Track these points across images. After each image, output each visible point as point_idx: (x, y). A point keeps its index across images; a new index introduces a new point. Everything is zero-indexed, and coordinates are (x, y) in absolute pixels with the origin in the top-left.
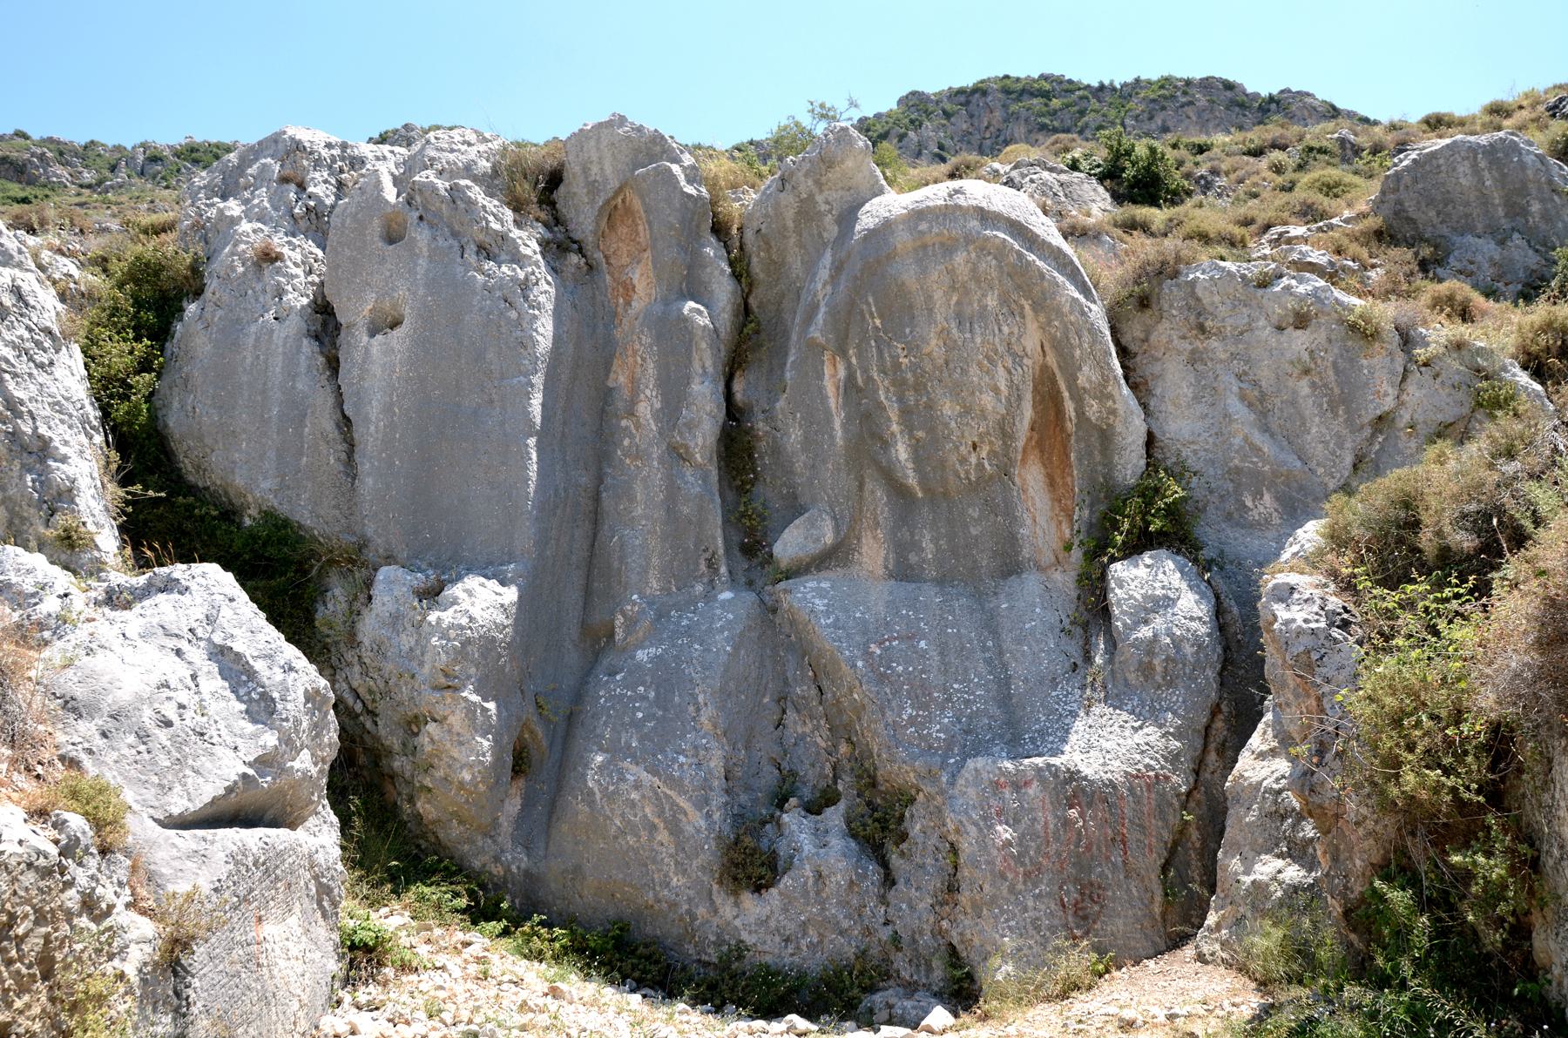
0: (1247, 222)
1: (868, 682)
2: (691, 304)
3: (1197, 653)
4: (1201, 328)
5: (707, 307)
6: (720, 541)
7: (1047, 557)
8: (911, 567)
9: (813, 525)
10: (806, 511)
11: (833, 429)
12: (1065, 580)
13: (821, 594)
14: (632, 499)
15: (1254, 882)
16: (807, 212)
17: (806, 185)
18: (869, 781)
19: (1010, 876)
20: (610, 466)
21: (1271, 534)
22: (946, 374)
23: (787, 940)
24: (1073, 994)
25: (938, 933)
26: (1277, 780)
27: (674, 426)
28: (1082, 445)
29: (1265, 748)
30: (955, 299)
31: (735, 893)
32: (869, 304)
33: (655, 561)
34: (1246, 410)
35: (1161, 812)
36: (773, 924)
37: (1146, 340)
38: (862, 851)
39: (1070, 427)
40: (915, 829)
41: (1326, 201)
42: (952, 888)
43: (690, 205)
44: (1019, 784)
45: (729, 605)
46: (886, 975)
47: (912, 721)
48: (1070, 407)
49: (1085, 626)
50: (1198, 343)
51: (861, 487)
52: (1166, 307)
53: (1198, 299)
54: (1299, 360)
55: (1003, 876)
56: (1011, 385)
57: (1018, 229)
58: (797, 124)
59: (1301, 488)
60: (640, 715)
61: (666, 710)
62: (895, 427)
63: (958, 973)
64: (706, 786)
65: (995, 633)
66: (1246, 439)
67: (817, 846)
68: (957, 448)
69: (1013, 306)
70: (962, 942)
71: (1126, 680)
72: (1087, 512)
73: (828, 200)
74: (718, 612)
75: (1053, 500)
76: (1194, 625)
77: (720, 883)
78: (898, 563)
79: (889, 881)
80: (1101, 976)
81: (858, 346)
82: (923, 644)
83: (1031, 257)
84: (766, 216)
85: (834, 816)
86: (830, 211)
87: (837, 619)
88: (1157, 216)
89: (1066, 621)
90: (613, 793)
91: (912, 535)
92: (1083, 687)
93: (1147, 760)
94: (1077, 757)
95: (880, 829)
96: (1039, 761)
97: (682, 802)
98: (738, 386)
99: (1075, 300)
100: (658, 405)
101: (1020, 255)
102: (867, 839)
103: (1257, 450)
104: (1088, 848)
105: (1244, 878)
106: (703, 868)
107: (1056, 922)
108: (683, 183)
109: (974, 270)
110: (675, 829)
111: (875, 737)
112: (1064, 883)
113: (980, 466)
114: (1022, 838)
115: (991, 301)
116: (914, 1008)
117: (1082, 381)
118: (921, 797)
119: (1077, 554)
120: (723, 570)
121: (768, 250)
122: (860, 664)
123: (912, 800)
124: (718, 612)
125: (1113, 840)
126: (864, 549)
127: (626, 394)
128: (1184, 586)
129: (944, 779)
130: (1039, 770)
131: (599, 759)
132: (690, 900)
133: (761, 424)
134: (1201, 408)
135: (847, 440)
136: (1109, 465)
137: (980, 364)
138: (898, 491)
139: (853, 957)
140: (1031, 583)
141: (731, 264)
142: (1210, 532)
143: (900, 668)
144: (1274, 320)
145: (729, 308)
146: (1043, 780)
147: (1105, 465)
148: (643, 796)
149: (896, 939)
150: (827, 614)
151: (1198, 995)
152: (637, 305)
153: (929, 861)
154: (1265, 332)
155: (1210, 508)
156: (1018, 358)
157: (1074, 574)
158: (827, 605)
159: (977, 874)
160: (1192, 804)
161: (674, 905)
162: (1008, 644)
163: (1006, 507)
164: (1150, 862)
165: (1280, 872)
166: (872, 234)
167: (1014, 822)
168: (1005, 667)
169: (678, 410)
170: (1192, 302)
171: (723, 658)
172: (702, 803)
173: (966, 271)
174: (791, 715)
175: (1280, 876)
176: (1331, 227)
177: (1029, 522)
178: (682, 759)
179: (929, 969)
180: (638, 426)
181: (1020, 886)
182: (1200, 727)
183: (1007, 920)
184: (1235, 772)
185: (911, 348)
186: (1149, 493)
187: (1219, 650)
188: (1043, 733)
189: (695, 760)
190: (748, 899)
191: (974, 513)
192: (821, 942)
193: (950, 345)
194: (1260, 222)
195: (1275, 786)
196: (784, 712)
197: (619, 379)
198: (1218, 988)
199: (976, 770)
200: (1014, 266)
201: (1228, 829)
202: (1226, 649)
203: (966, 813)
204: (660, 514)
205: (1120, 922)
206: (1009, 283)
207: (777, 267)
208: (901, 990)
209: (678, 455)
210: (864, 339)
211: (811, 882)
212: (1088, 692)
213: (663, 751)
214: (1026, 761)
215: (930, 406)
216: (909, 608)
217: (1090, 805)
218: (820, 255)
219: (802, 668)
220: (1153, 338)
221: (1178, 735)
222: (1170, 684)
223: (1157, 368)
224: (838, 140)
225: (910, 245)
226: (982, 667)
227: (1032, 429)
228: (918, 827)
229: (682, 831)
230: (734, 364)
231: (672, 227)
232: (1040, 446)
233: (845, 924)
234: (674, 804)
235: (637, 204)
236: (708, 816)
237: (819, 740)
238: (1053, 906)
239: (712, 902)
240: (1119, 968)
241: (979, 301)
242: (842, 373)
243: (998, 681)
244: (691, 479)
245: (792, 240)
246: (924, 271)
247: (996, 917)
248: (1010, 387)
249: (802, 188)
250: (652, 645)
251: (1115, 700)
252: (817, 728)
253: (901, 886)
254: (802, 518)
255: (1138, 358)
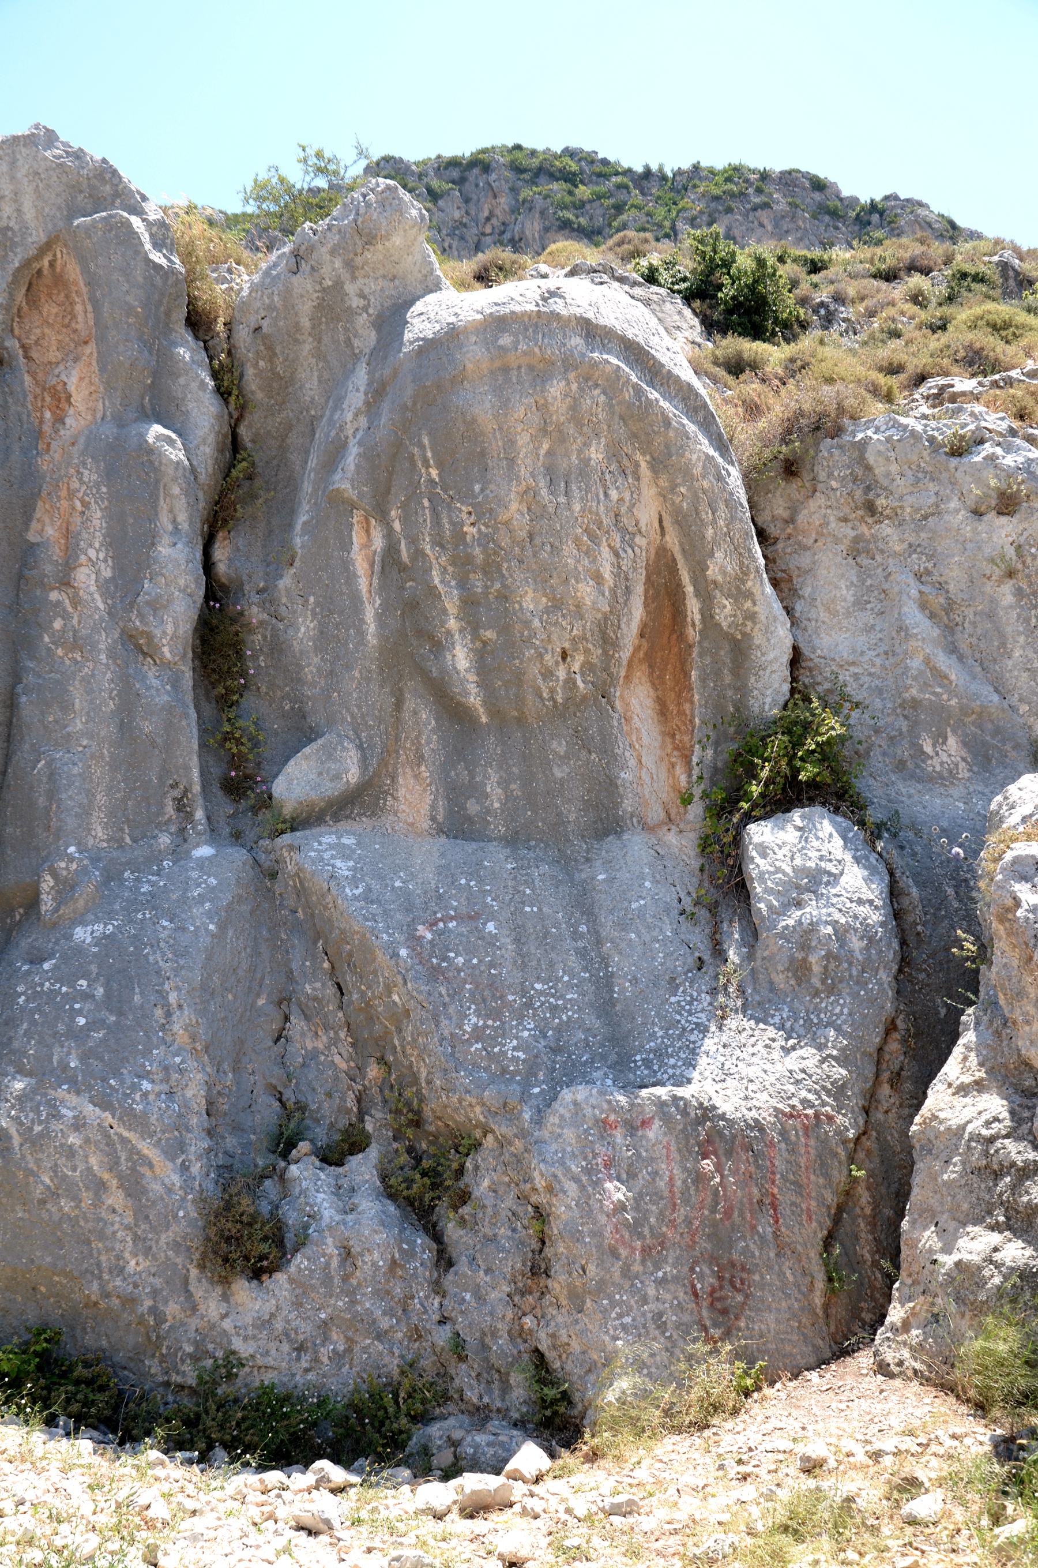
0: (893, 369)
1: (416, 979)
2: (157, 429)
3: (867, 948)
4: (871, 508)
5: (180, 435)
6: (195, 774)
7: (655, 813)
8: (469, 819)
9: (330, 757)
10: (319, 735)
11: (362, 621)
12: (682, 844)
13: (345, 853)
14: (66, 707)
15: (958, 1264)
16: (331, 307)
17: (332, 267)
18: (411, 1118)
19: (624, 1252)
20: (32, 658)
21: (956, 792)
22: (529, 553)
23: (300, 1349)
24: (715, 1421)
25: (519, 1334)
26: (988, 1124)
27: (132, 604)
28: (708, 660)
29: (967, 1079)
30: (546, 446)
31: (225, 1281)
32: (422, 447)
33: (101, 799)
34: (928, 622)
35: (823, 1164)
36: (279, 1325)
37: (791, 520)
38: (405, 1217)
39: (692, 634)
40: (482, 1187)
41: (1000, 347)
42: (538, 1270)
43: (158, 281)
44: (634, 1126)
45: (210, 866)
46: (445, 1397)
47: (478, 1034)
48: (693, 607)
49: (713, 909)
50: (864, 529)
51: (399, 705)
52: (822, 475)
53: (868, 468)
54: (1003, 557)
55: (614, 1254)
56: (618, 571)
57: (636, 354)
58: (282, 180)
59: (997, 731)
60: (82, 1021)
61: (120, 1013)
62: (452, 624)
63: (551, 1393)
64: (181, 1125)
65: (590, 914)
66: (927, 661)
67: (341, 1211)
68: (541, 656)
69: (625, 462)
70: (555, 1347)
71: (771, 983)
72: (710, 753)
73: (362, 292)
74: (194, 874)
75: (664, 734)
76: (863, 910)
77: (202, 1267)
78: (450, 813)
79: (444, 1260)
80: (747, 1394)
81: (404, 506)
82: (491, 927)
83: (654, 395)
84: (271, 308)
85: (363, 1168)
86: (365, 309)
87: (369, 889)
88: (773, 354)
89: (687, 903)
90: (41, 1135)
91: (472, 775)
92: (713, 992)
93: (803, 1094)
94: (710, 1087)
95: (428, 1187)
96: (662, 1092)
97: (146, 1147)
98: (221, 553)
99: (709, 458)
100: (107, 573)
101: (638, 391)
102: (410, 1201)
103: (941, 677)
104: (728, 1213)
105: (942, 1258)
106: (176, 1246)
107: (686, 1318)
108: (148, 246)
109: (574, 408)
110: (134, 1187)
111: (425, 1056)
112: (696, 1263)
113: (570, 682)
114: (638, 1199)
115: (596, 454)
116: (489, 1444)
117: (713, 572)
118: (489, 1141)
119: (696, 809)
120: (199, 814)
121: (272, 357)
122: (403, 952)
123: (477, 1146)
124: (194, 874)
125: (760, 1202)
126: (402, 792)
127: (57, 553)
128: (848, 857)
129: (527, 1116)
130: (661, 1104)
131: (19, 1085)
132: (155, 1293)
133: (255, 609)
134: (867, 617)
135: (381, 636)
136: (742, 689)
137: (577, 541)
138: (452, 711)
139: (396, 1372)
140: (636, 846)
141: (215, 375)
142: (875, 786)
143: (460, 960)
144: (971, 502)
145: (211, 439)
146: (667, 1120)
147: (737, 689)
148: (87, 1141)
149: (458, 1345)
150: (354, 882)
151: (895, 1422)
152: (75, 422)
153: (503, 1231)
154: (957, 516)
155: (876, 754)
156: (629, 536)
157: (693, 836)
158: (354, 869)
159: (579, 1249)
160: (861, 1155)
161: (130, 1301)
162: (608, 930)
163: (603, 741)
164: (807, 1233)
165: (996, 1250)
166: (429, 347)
167: (628, 1177)
168: (605, 961)
169: (138, 581)
170: (859, 472)
171: (205, 941)
172: (175, 1149)
173: (563, 409)
174: (297, 1024)
175: (997, 1257)
176: (1010, 382)
177: (632, 762)
178: (146, 1085)
179: (506, 1388)
180: (76, 602)
181: (637, 1268)
182: (872, 1049)
183: (620, 1316)
184: (924, 1110)
185: (482, 512)
186: (798, 730)
187: (895, 945)
188: (660, 1053)
189: (165, 1087)
190: (243, 1289)
191: (560, 747)
192: (349, 1350)
193: (537, 512)
194: (910, 369)
195: (985, 1132)
196: (287, 1019)
197: (46, 530)
198: (918, 1412)
199: (575, 1103)
200: (630, 405)
201: (915, 1191)
202: (903, 943)
203: (563, 1164)
204: (108, 731)
205: (771, 1318)
206: (621, 431)
207: (282, 385)
208: (466, 1419)
209: (137, 646)
210: (413, 497)
211: (335, 1262)
212: (721, 999)
213: (117, 1074)
214: (644, 1092)
215: (504, 597)
216: (470, 876)
217: (729, 1154)
218: (348, 372)
219: (314, 958)
220: (802, 518)
221: (842, 1060)
222: (831, 990)
223: (805, 560)
224: (382, 204)
225: (485, 366)
226: (573, 961)
227: (642, 635)
228: (486, 1183)
229: (145, 1191)
230: (216, 521)
231: (130, 311)
232: (649, 659)
233: (385, 1323)
234: (133, 1151)
235: (73, 271)
236: (184, 1168)
237: (337, 1059)
238: (681, 1295)
239: (189, 1295)
240: (772, 1383)
241: (580, 452)
242: (378, 543)
243: (595, 979)
244: (155, 683)
245: (307, 348)
246: (505, 404)
247: (605, 1312)
248: (617, 575)
249: (326, 270)
250: (97, 920)
251: (758, 1010)
252: (335, 1042)
253: (463, 1266)
254: (314, 746)
255: (780, 545)
